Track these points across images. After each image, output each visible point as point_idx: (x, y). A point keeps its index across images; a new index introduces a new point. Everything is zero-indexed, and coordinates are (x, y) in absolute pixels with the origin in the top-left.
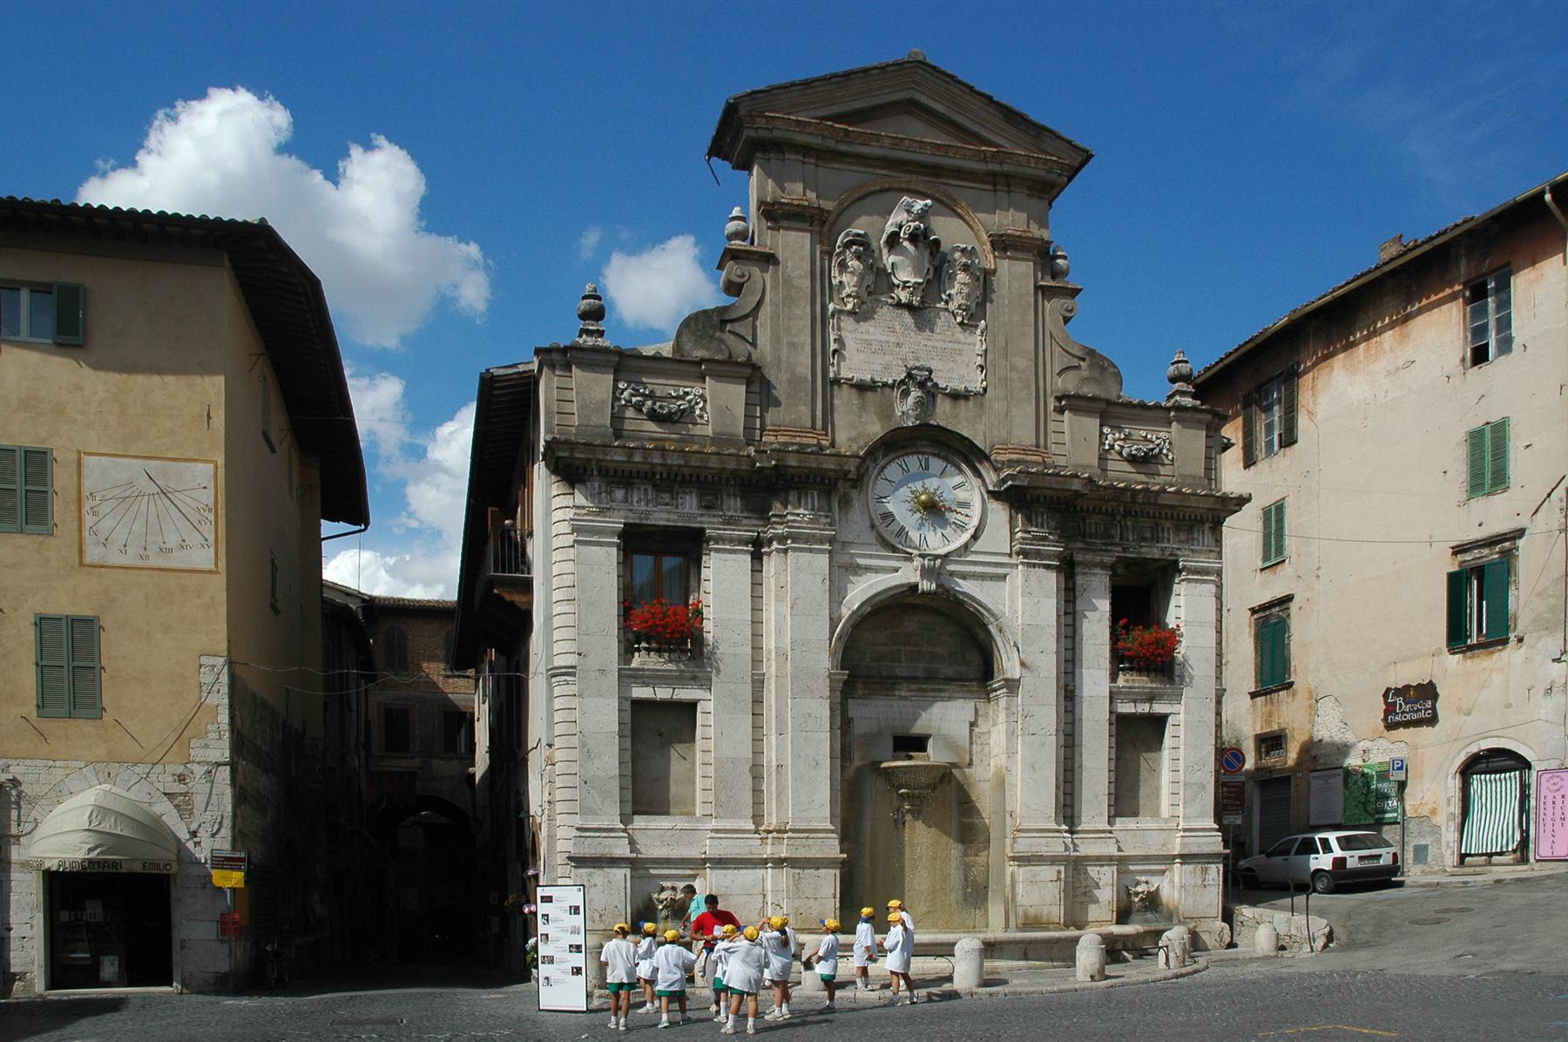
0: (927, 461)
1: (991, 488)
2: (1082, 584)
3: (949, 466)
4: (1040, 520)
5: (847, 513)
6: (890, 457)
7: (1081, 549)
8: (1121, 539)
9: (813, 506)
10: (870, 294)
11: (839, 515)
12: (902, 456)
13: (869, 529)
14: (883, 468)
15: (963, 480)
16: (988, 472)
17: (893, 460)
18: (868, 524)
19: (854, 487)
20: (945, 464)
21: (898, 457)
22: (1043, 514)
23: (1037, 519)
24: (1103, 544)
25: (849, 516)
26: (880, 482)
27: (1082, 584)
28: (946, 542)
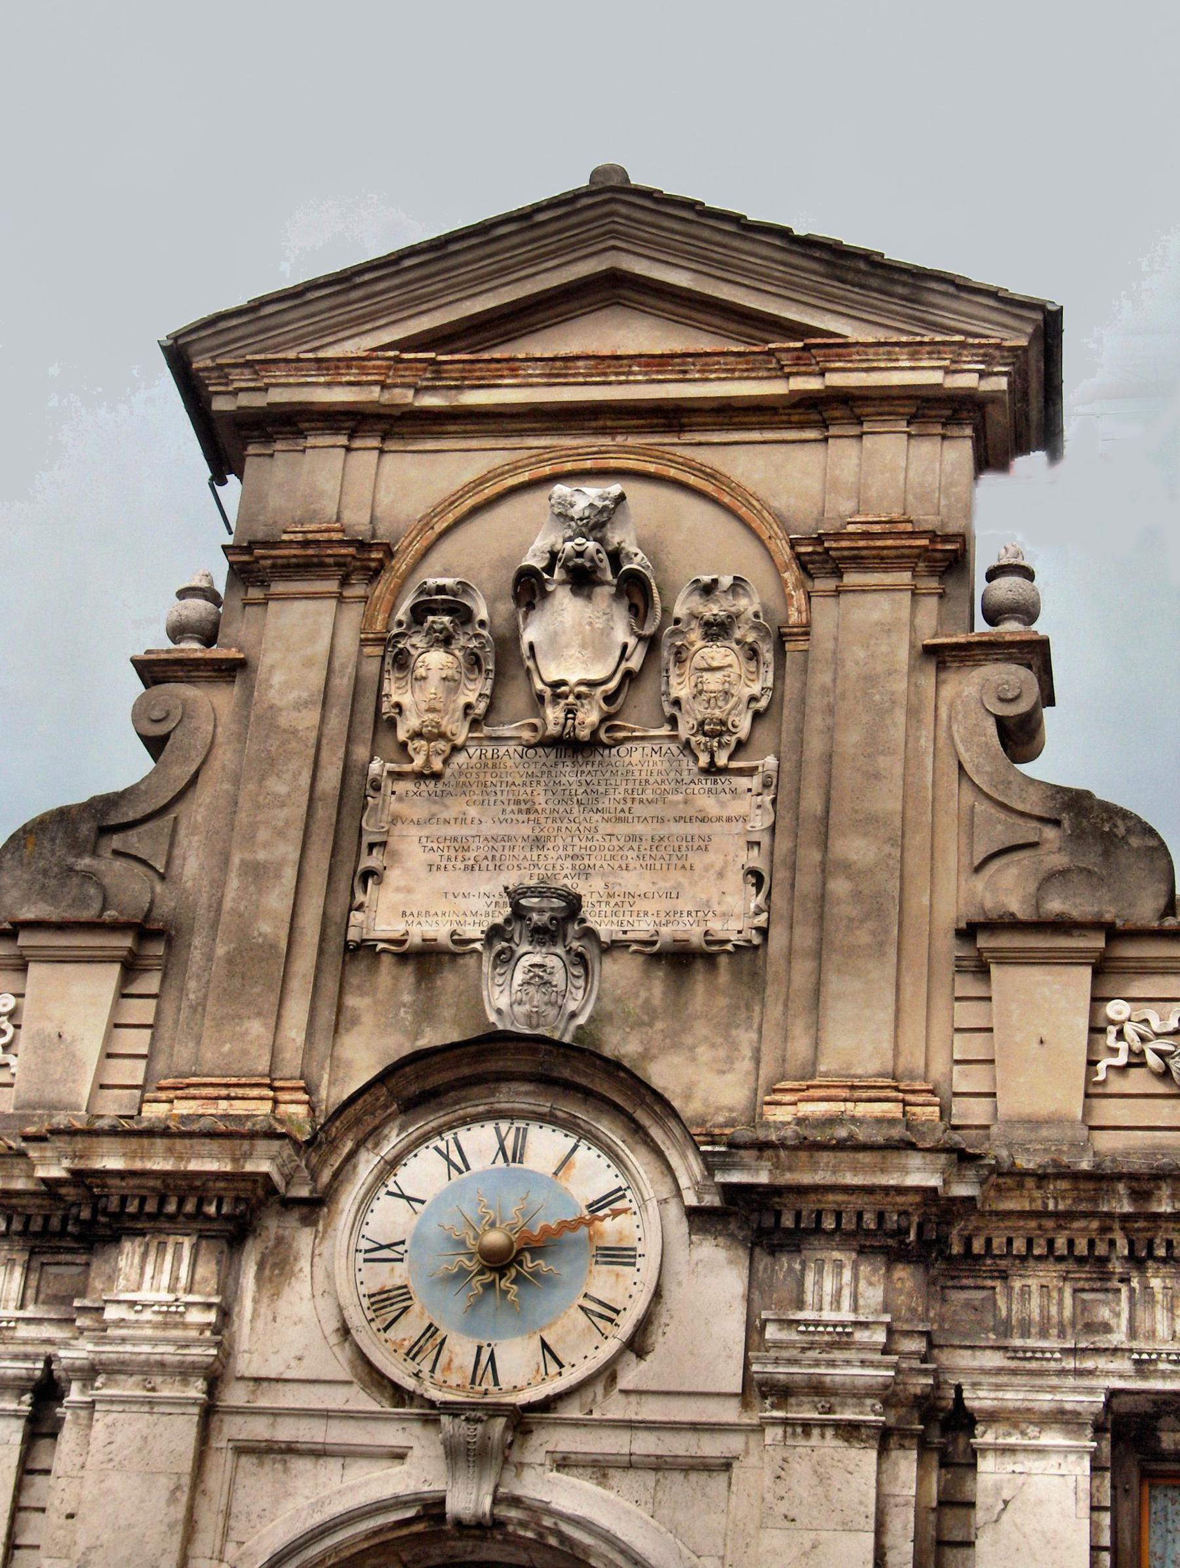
0: (521, 1135)
1: (691, 1199)
2: (998, 1489)
3: (583, 1144)
4: (829, 1285)
5: (276, 1295)
6: (414, 1130)
7: (999, 1371)
8: (1133, 1333)
9: (175, 1279)
10: (475, 724)
11: (256, 1301)
12: (450, 1126)
13: (334, 1339)
14: (392, 1165)
15: (621, 1182)
16: (684, 1156)
17: (424, 1139)
18: (334, 1324)
19: (309, 1220)
20: (571, 1142)
21: (439, 1132)
22: (839, 1265)
23: (819, 1284)
24: (1065, 1351)
25: (282, 1305)
26: (384, 1204)
27: (998, 1489)
28: (553, 1368)
